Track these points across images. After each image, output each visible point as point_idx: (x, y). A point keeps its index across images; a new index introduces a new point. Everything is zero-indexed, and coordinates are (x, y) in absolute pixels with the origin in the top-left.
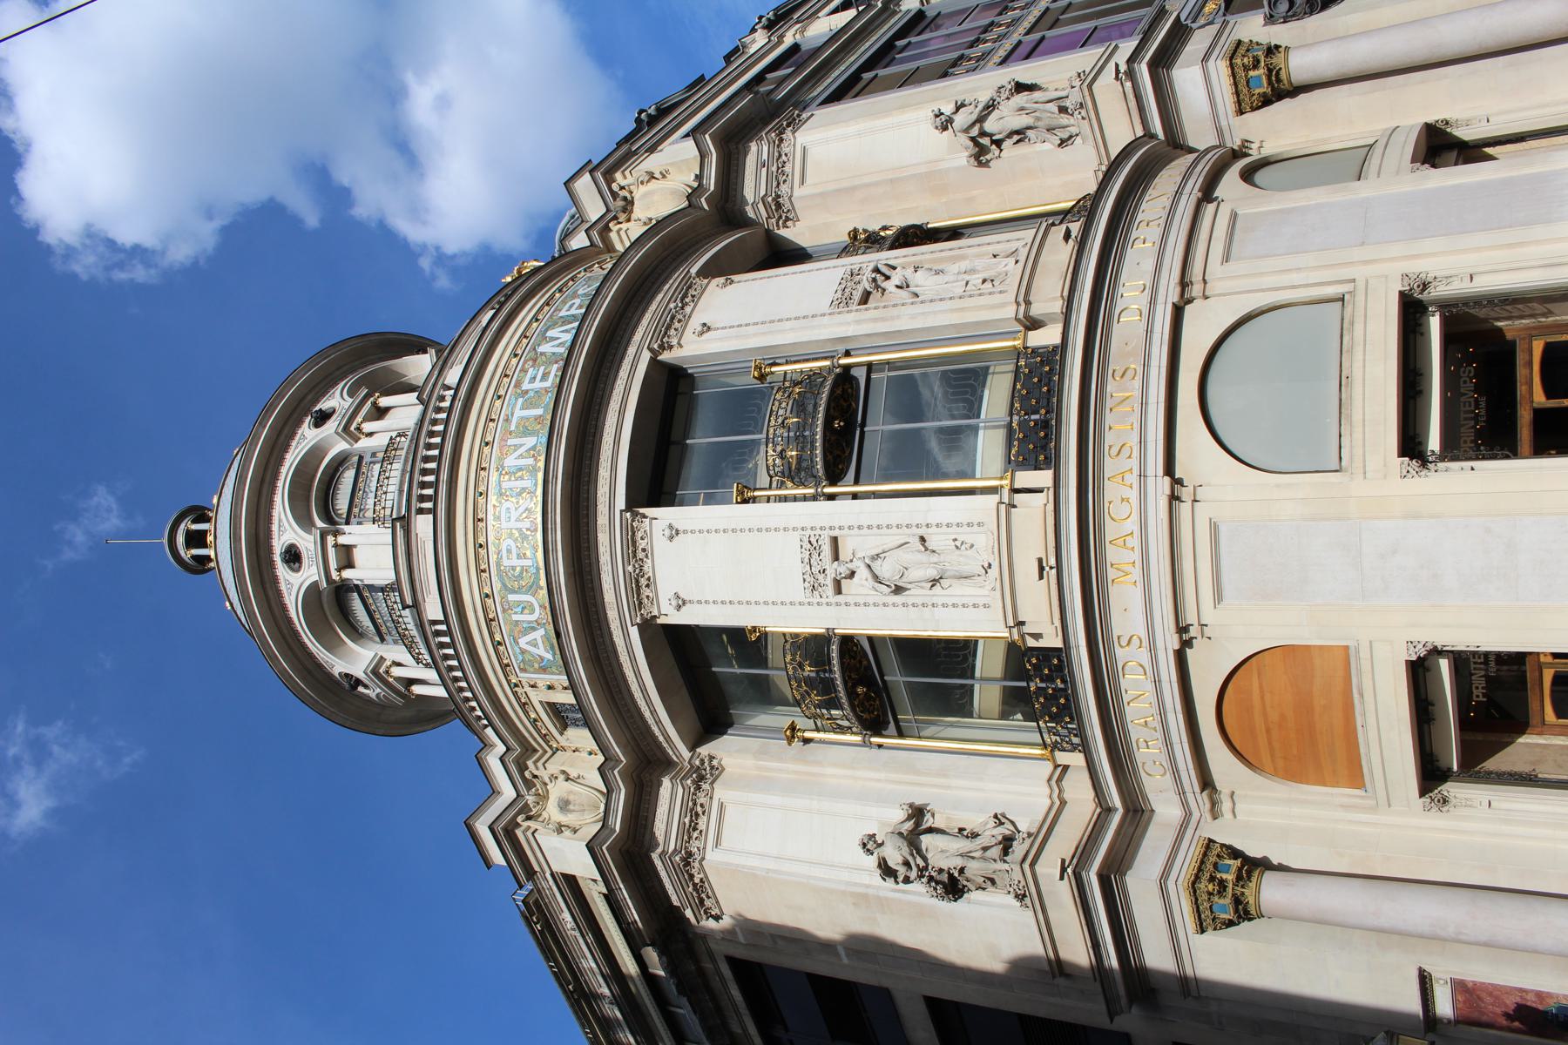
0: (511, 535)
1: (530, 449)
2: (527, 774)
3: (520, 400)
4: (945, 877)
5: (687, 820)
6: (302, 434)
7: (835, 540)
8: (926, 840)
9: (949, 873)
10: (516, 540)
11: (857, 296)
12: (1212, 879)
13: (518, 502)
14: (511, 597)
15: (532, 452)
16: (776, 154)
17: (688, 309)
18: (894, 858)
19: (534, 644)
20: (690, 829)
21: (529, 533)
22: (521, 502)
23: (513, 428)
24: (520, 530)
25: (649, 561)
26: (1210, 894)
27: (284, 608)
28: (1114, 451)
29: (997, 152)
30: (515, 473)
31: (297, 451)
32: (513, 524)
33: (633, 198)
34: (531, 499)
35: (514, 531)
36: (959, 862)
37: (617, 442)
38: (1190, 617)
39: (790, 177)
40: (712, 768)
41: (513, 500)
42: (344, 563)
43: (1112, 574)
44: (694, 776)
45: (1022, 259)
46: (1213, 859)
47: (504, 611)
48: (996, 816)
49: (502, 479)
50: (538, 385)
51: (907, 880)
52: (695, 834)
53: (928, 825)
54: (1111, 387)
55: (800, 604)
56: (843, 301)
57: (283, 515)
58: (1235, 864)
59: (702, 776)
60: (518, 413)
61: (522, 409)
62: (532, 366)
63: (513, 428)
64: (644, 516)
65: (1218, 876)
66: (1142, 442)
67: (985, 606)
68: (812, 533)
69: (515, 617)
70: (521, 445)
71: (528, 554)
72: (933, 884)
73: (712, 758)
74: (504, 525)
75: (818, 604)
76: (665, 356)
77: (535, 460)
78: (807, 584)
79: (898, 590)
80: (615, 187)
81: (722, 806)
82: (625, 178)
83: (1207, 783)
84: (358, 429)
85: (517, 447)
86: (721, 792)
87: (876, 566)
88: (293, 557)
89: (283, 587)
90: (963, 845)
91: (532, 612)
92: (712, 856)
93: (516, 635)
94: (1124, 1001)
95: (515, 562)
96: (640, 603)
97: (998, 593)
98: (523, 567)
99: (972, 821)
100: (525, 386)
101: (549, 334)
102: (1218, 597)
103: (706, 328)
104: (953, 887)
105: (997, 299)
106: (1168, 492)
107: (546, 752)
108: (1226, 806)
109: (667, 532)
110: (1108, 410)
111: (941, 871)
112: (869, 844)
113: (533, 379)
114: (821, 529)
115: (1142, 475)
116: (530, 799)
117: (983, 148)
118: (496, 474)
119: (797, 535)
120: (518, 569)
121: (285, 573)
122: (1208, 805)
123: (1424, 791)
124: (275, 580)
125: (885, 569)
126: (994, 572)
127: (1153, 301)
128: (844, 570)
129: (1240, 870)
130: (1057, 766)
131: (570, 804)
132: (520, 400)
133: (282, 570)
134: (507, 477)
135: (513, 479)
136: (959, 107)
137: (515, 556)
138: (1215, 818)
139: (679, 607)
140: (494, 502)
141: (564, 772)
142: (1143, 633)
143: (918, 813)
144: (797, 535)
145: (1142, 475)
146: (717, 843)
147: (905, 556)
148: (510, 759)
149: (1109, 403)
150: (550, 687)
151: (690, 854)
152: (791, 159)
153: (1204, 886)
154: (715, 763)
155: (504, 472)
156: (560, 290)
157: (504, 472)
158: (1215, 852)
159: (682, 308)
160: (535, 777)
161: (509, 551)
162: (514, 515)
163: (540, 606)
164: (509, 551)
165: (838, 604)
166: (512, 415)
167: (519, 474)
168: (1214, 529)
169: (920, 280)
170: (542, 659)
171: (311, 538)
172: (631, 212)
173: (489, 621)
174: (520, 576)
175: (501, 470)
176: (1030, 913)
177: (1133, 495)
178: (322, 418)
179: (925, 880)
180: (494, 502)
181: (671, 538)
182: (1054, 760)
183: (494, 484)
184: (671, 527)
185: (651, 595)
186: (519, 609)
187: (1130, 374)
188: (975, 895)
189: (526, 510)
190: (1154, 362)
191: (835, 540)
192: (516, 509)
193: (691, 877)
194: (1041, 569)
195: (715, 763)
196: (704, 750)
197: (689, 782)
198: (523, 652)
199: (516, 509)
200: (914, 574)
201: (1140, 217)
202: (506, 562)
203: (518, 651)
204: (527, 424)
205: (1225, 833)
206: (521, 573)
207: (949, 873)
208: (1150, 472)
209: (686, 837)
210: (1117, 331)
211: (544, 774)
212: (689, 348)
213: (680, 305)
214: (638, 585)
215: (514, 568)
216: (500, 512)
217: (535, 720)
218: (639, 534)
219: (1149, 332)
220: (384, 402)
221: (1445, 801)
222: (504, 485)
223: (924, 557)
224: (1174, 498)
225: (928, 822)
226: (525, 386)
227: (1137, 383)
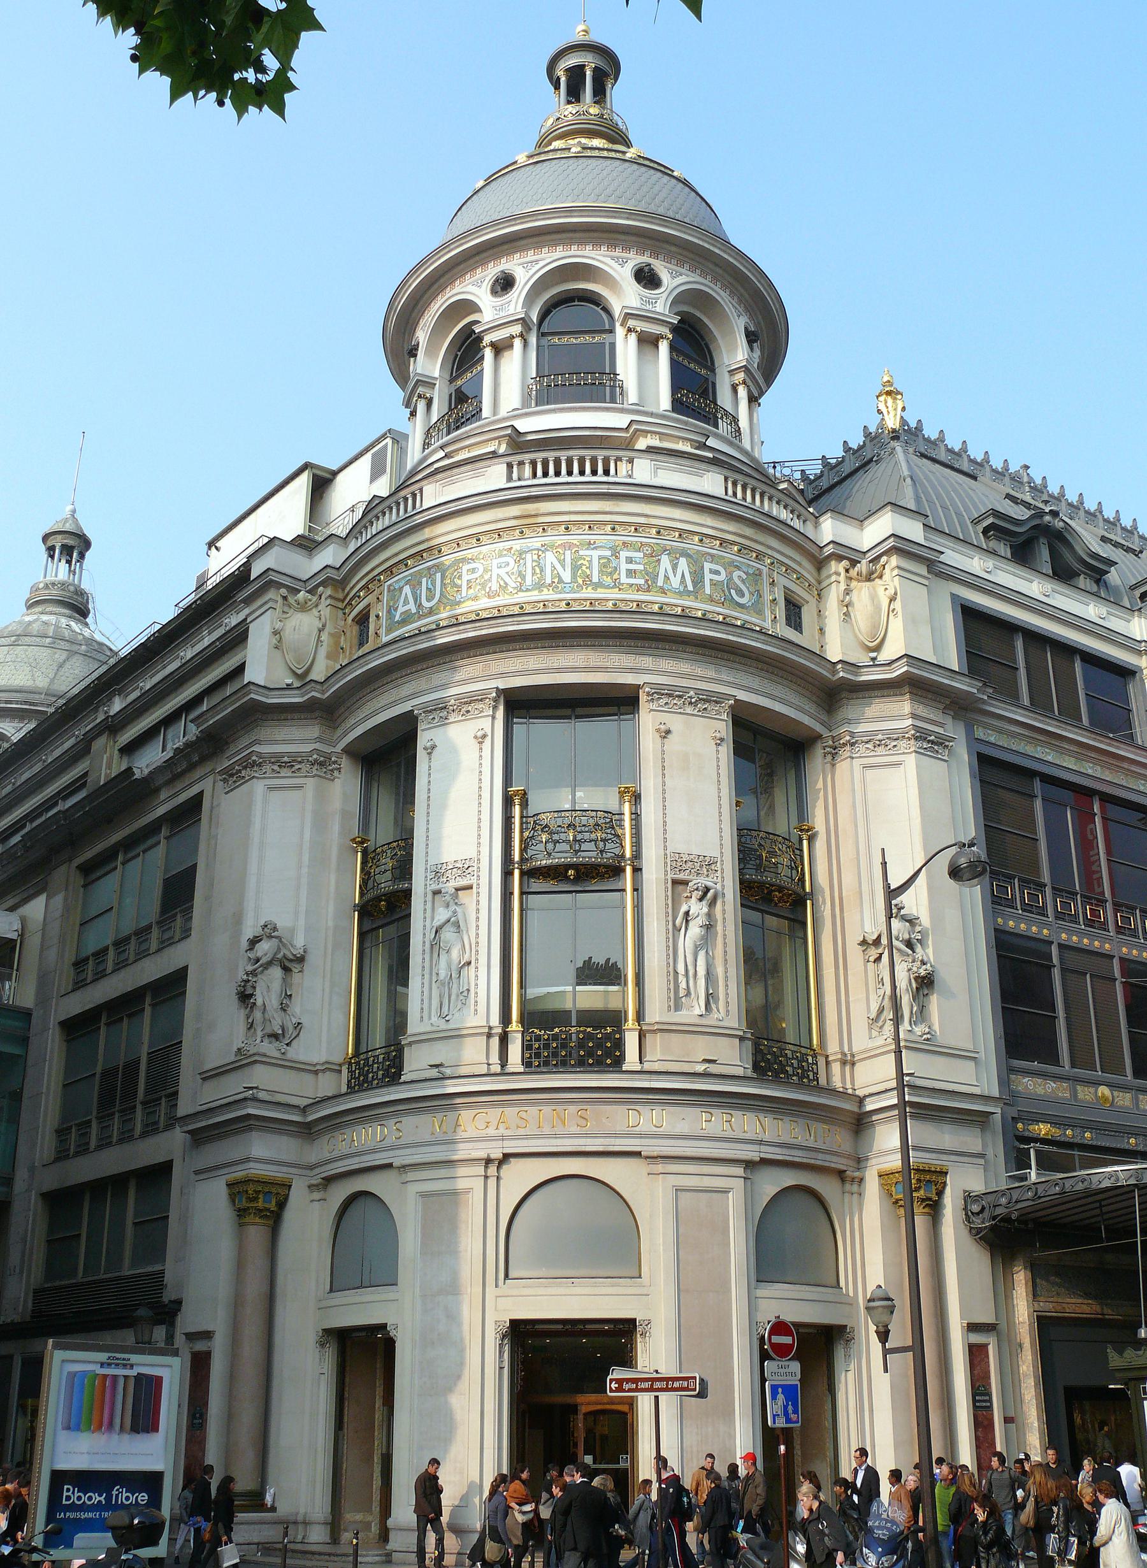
0: (486, 571)
1: (559, 577)
2: (321, 589)
3: (609, 553)
4: (249, 991)
5: (286, 759)
6: (628, 259)
7: (470, 887)
8: (276, 972)
9: (252, 995)
10: (481, 576)
11: (682, 876)
12: (258, 1192)
13: (513, 573)
14: (438, 575)
15: (556, 580)
16: (895, 736)
17: (689, 710)
18: (265, 948)
19: (406, 602)
21: (487, 590)
22: (513, 577)
23: (581, 553)
24: (490, 580)
25: (460, 718)
26: (247, 1191)
28: (523, 1114)
29: (872, 959)
30: (538, 566)
31: (608, 260)
32: (495, 571)
33: (874, 580)
34: (514, 588)
35: (489, 573)
36: (259, 1002)
37: (559, 670)
38: (411, 1176)
39: (872, 753)
40: (332, 770)
41: (516, 568)
42: (500, 346)
43: (440, 1115)
44: (322, 759)
45: (704, 1021)
46: (274, 1190)
47: (429, 568)
48: (299, 1023)
49: (534, 552)
50: (624, 567)
52: (276, 767)
53: (293, 969)
54: (572, 1109)
55: (427, 861)
56: (677, 862)
57: (542, 264)
58: (273, 1206)
59: (323, 764)
60: (595, 554)
61: (600, 558)
62: (645, 555)
63: (581, 553)
64: (495, 708)
65: (260, 1196)
66: (526, 1137)
67: (422, 1017)
68: (475, 869)
69: (424, 580)
70: (563, 567)
71: (471, 591)
72: (243, 984)
73: (339, 770)
74: (495, 562)
75: (426, 877)
76: (643, 698)
77: (549, 585)
78: (439, 866)
80: (884, 559)
81: (299, 787)
82: (893, 569)
83: (329, 1180)
84: (630, 330)
85: (562, 563)
86: (310, 783)
87: (448, 927)
88: (505, 284)
90: (273, 1002)
91: (428, 600)
93: (412, 582)
94: (186, 1129)
95: (465, 578)
96: (430, 711)
97: (429, 1029)
98: (460, 586)
99: (296, 1007)
100: (624, 554)
101: (683, 561)
102: (424, 1195)
104: (245, 997)
106: (493, 1156)
107: (343, 601)
108: (316, 1195)
109: (480, 734)
110: (554, 1108)
111: (254, 988)
113: (630, 560)
114: (478, 876)
115: (503, 1138)
116: (302, 595)
118: (538, 545)
119: (474, 855)
120: (459, 582)
121: (490, 276)
122: (314, 1182)
123: (328, 1332)
124: (484, 263)
126: (443, 1025)
127: (641, 1136)
129: (268, 1210)
130: (340, 1065)
132: (609, 553)
133: (492, 271)
134: (535, 557)
135: (534, 564)
137: (469, 577)
138: (309, 1187)
139: (425, 749)
140: (515, 547)
141: (324, 626)
142: (401, 1142)
143: (301, 960)
144: (474, 855)
145: (503, 1138)
146: (271, 788)
148: (331, 573)
149: (559, 1108)
150: (377, 616)
151: (260, 765)
152: (891, 752)
153: (251, 1189)
154: (336, 773)
155: (540, 553)
156: (743, 548)
157: (540, 553)
158: (280, 1191)
159: (691, 703)
160: (320, 596)
161: (473, 571)
162: (502, 572)
163: (431, 608)
164: (473, 571)
165: (426, 894)
166: (595, 548)
167: (538, 570)
170: (396, 610)
171: (519, 309)
172: (859, 581)
173: (420, 554)
175: (543, 549)
176: (233, 1059)
177: (491, 1131)
178: (647, 278)
179: (245, 977)
180: (515, 547)
181: (476, 737)
182: (344, 1064)
183: (529, 545)
184: (484, 736)
185: (436, 721)
186: (430, 586)
187: (583, 1122)
188: (243, 1013)
189: (506, 583)
190: (589, 1141)
191: (470, 887)
192: (507, 573)
193: (245, 768)
194: (437, 1066)
195: (336, 773)
196: (345, 762)
197: (315, 756)
198: (401, 589)
199: (507, 573)
201: (737, 1114)
202: (465, 567)
203: (401, 584)
204: (584, 568)
205: (298, 1196)
206: (456, 586)
207: (252, 995)
208: (506, 1143)
209: (273, 760)
210: (621, 1109)
211: (324, 602)
212: (648, 718)
213: (693, 700)
214: (440, 710)
215: (460, 577)
216: (505, 555)
217: (359, 597)
218: (480, 706)
219: (616, 1136)
220: (664, 347)
221: (322, 1345)
222: (529, 556)
223: (454, 967)
225: (296, 967)
226: (624, 554)
227: (574, 1129)
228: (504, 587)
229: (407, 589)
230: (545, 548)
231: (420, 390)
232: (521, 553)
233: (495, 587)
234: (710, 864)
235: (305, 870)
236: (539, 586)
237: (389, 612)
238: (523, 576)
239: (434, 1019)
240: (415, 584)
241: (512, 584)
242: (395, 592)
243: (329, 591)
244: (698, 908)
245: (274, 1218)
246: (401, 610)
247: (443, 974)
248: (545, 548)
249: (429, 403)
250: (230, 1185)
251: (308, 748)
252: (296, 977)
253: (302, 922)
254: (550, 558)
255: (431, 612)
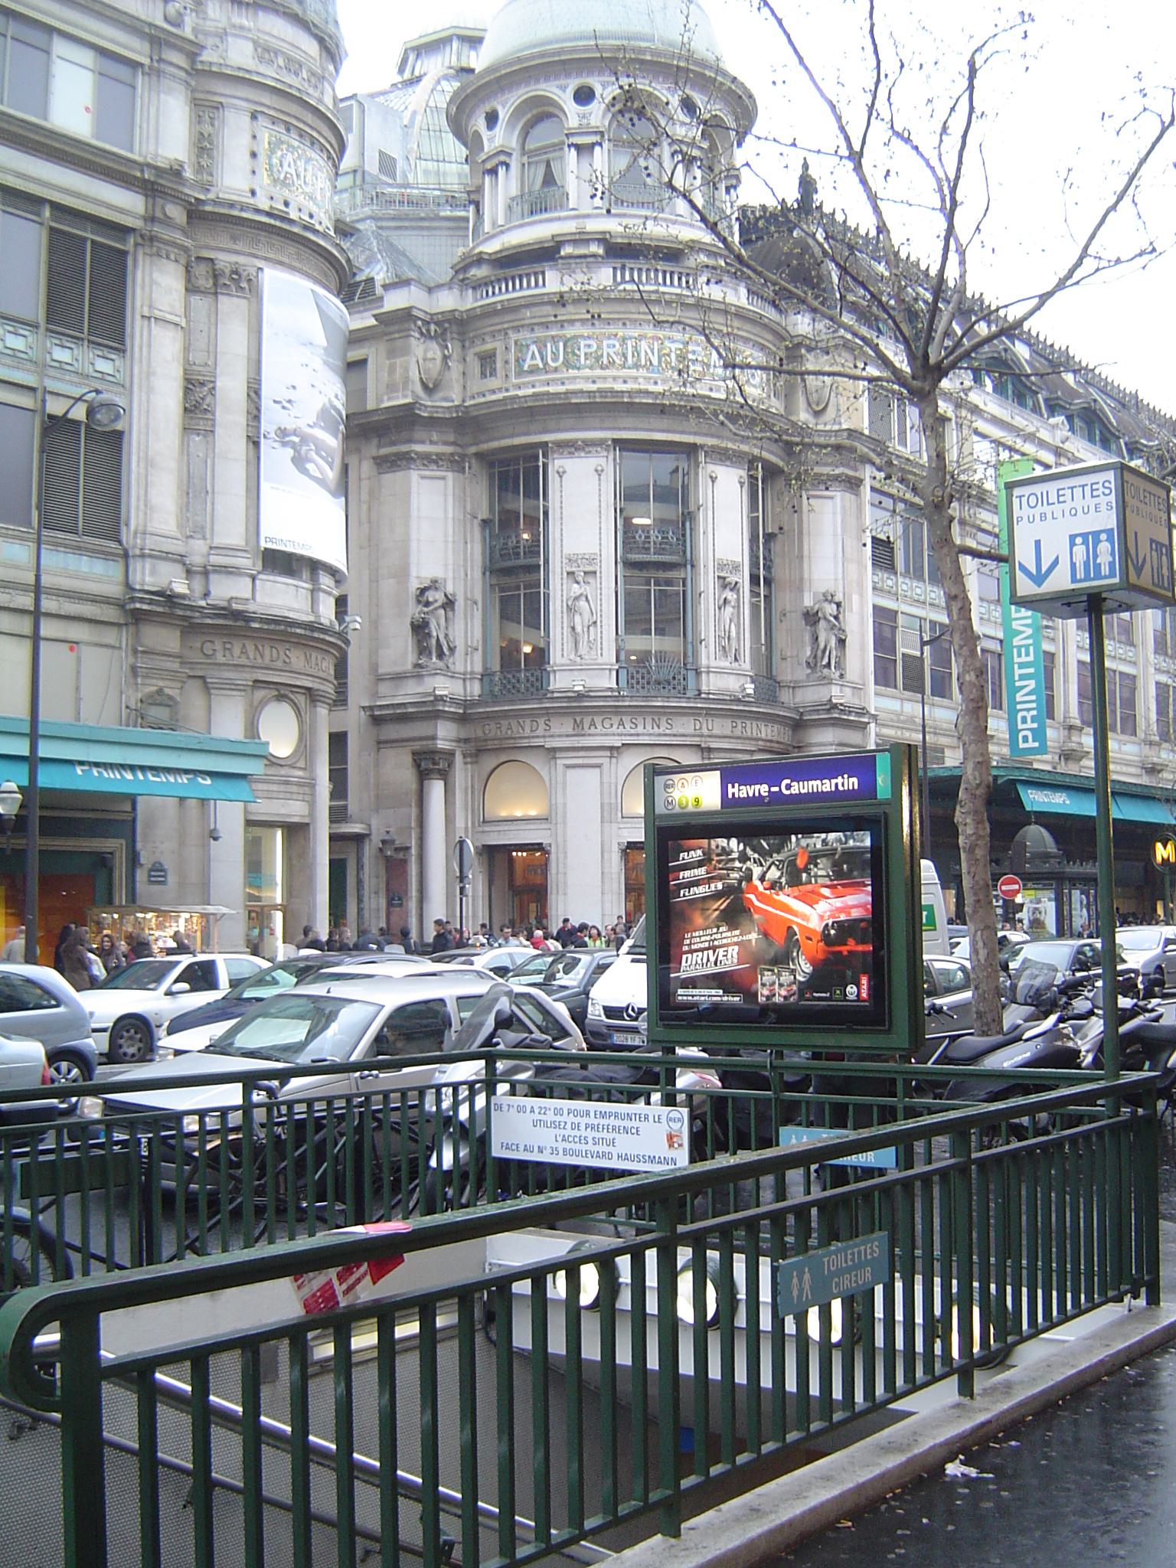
0: (599, 347)
8: (442, 612)
14: (561, 344)
18: (431, 596)
19: (533, 357)
20: (427, 459)
27: (547, 79)
47: (553, 337)
51: (419, 602)
59: (456, 463)
60: (673, 346)
79: (569, 609)
81: (443, 478)
86: (450, 475)
88: (584, 96)
89: (562, 82)
92: (414, 475)
95: (583, 350)
103: (713, 480)
105: (712, 656)
112: (434, 585)
117: (812, 618)
124: (568, 75)
125: (583, 603)
128: (580, 579)
131: (484, 521)
133: (573, 84)
136: (838, 605)
146: (423, 477)
147: (587, 614)
162: (611, 351)
164: (589, 346)
168: (599, 766)
169: (729, 610)
174: (574, 354)
191: (595, 573)
198: (528, 346)
200: (577, 618)
214: (571, 447)
223: (586, 623)
224: (611, 748)
228: (612, 363)
229: (533, 348)
230: (641, 337)
231: (502, 158)
232: (624, 340)
233: (605, 362)
234: (736, 568)
235: (450, 539)
236: (637, 366)
237: (517, 360)
238: (625, 356)
239: (572, 657)
240: (541, 344)
241: (618, 361)
242: (521, 347)
243: (454, 328)
244: (731, 596)
245: (445, 775)
246: (529, 362)
247: (579, 629)
248: (641, 337)
249: (507, 166)
250: (414, 753)
251: (449, 449)
252: (450, 614)
253: (451, 575)
254: (644, 345)
255: (556, 370)
